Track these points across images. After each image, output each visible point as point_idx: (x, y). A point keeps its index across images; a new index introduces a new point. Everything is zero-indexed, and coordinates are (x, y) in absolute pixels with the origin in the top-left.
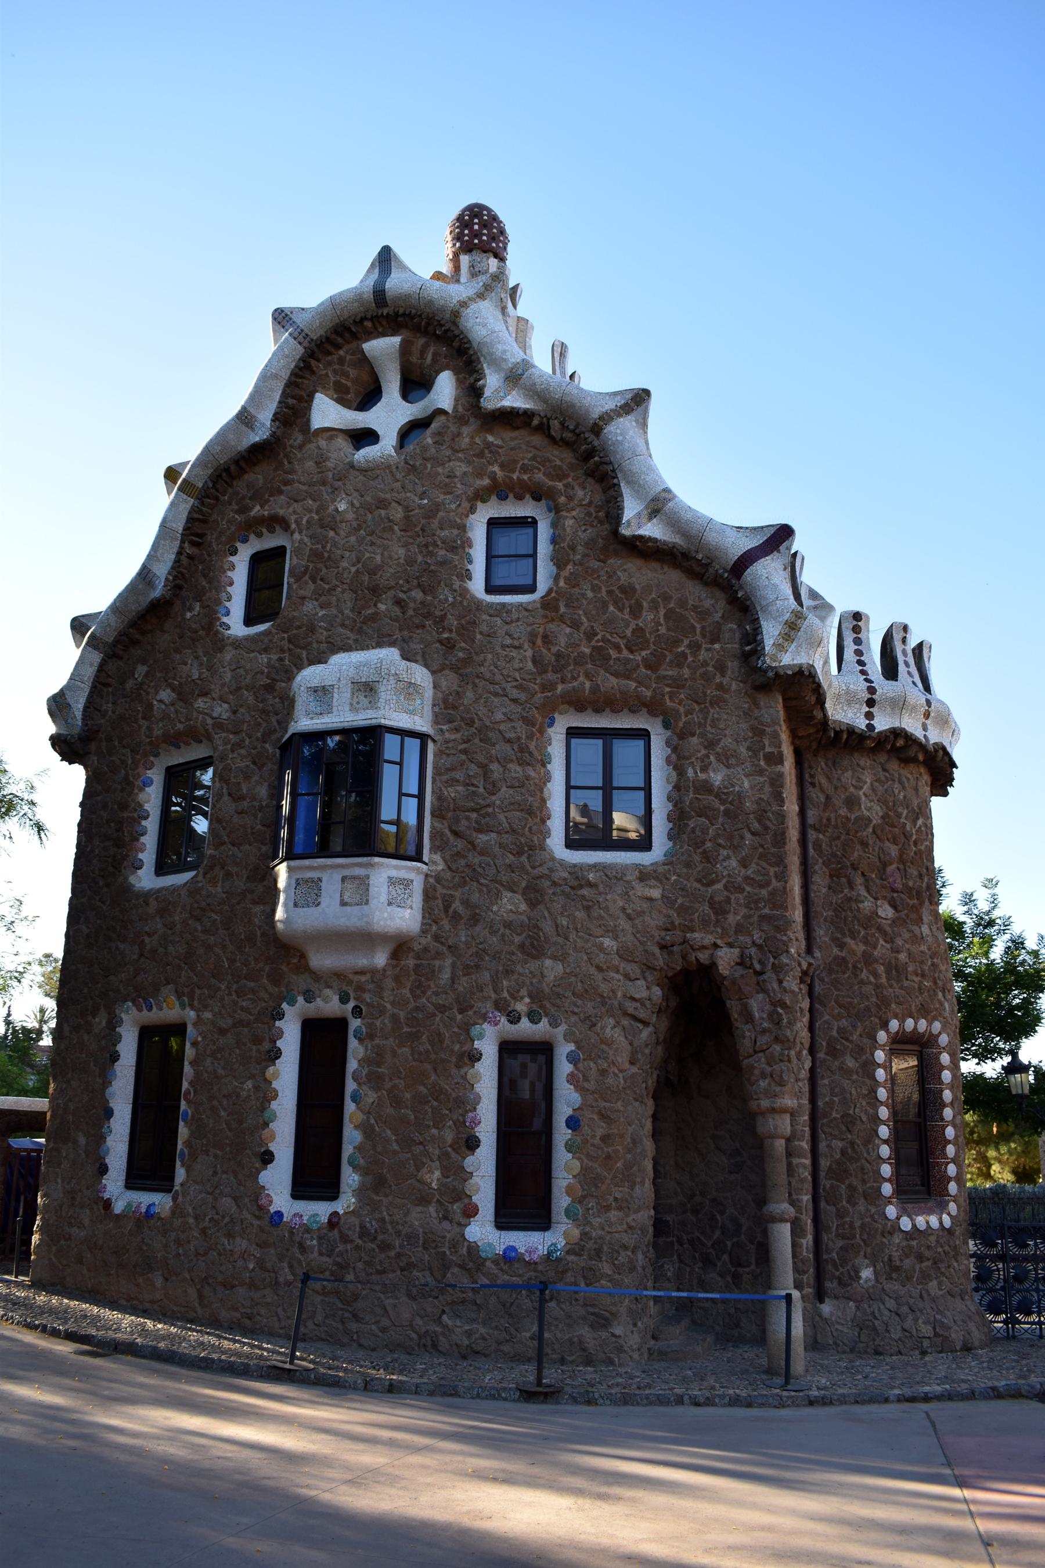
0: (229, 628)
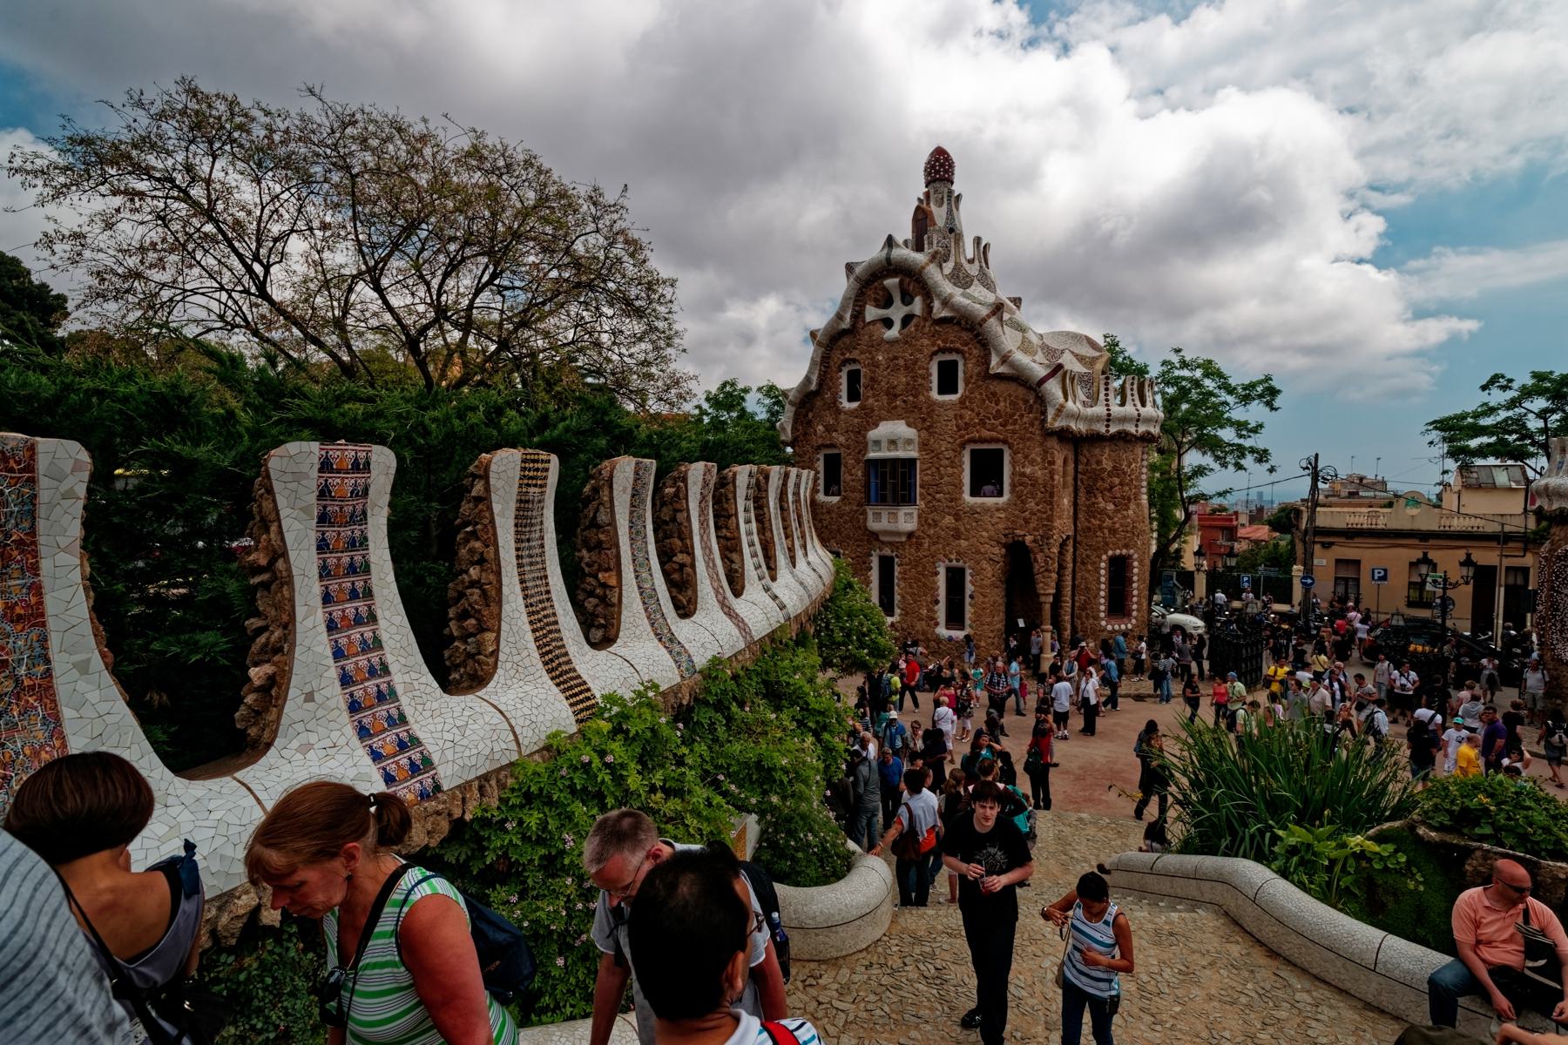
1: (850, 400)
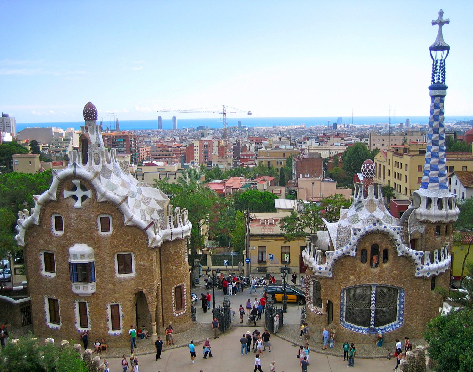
0: (53, 232)
1: (57, 229)
